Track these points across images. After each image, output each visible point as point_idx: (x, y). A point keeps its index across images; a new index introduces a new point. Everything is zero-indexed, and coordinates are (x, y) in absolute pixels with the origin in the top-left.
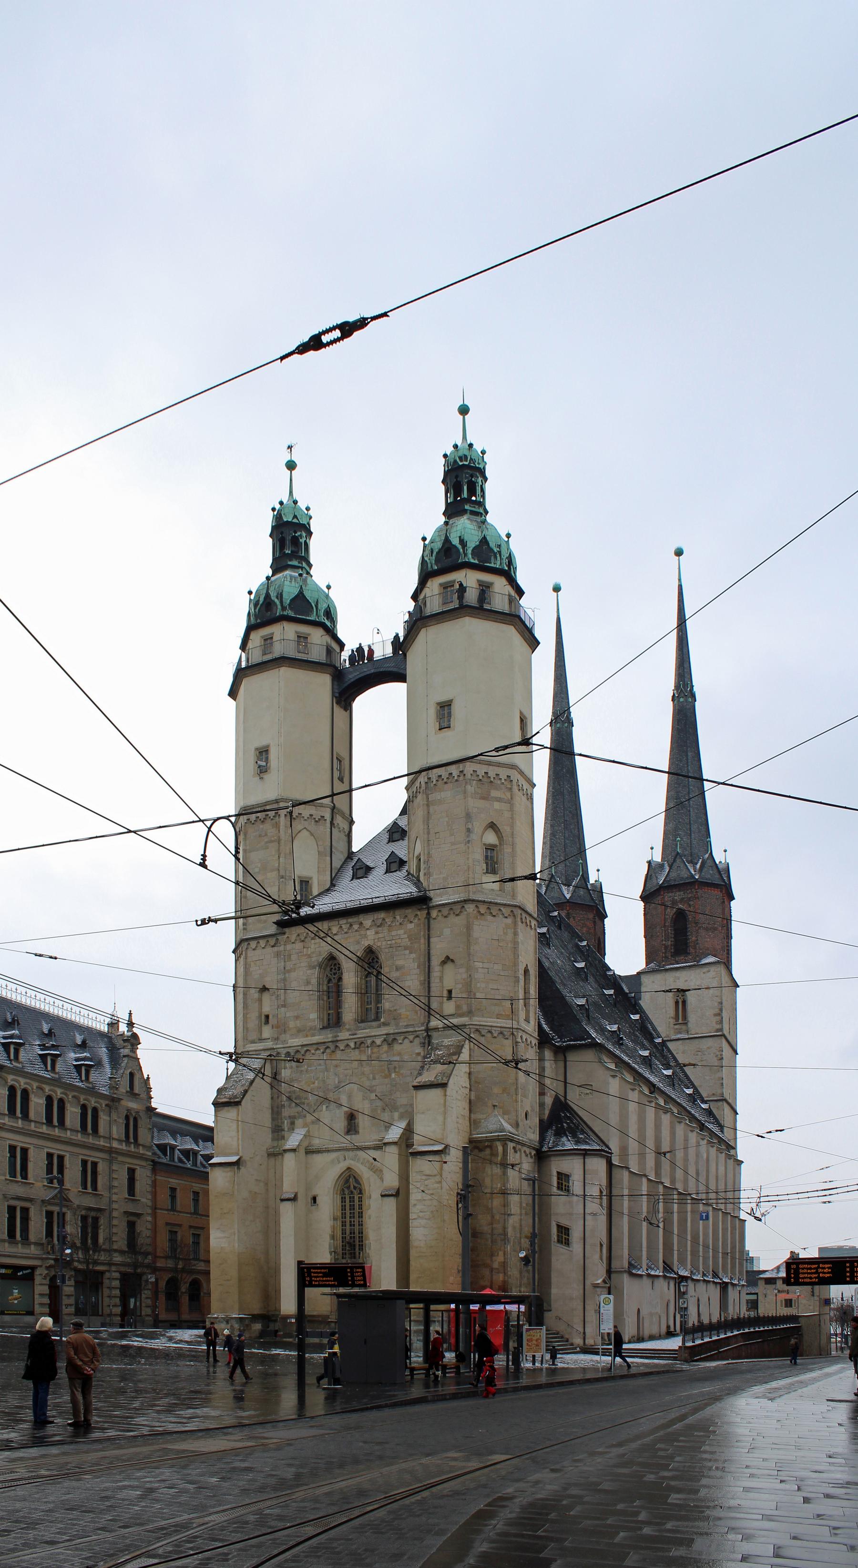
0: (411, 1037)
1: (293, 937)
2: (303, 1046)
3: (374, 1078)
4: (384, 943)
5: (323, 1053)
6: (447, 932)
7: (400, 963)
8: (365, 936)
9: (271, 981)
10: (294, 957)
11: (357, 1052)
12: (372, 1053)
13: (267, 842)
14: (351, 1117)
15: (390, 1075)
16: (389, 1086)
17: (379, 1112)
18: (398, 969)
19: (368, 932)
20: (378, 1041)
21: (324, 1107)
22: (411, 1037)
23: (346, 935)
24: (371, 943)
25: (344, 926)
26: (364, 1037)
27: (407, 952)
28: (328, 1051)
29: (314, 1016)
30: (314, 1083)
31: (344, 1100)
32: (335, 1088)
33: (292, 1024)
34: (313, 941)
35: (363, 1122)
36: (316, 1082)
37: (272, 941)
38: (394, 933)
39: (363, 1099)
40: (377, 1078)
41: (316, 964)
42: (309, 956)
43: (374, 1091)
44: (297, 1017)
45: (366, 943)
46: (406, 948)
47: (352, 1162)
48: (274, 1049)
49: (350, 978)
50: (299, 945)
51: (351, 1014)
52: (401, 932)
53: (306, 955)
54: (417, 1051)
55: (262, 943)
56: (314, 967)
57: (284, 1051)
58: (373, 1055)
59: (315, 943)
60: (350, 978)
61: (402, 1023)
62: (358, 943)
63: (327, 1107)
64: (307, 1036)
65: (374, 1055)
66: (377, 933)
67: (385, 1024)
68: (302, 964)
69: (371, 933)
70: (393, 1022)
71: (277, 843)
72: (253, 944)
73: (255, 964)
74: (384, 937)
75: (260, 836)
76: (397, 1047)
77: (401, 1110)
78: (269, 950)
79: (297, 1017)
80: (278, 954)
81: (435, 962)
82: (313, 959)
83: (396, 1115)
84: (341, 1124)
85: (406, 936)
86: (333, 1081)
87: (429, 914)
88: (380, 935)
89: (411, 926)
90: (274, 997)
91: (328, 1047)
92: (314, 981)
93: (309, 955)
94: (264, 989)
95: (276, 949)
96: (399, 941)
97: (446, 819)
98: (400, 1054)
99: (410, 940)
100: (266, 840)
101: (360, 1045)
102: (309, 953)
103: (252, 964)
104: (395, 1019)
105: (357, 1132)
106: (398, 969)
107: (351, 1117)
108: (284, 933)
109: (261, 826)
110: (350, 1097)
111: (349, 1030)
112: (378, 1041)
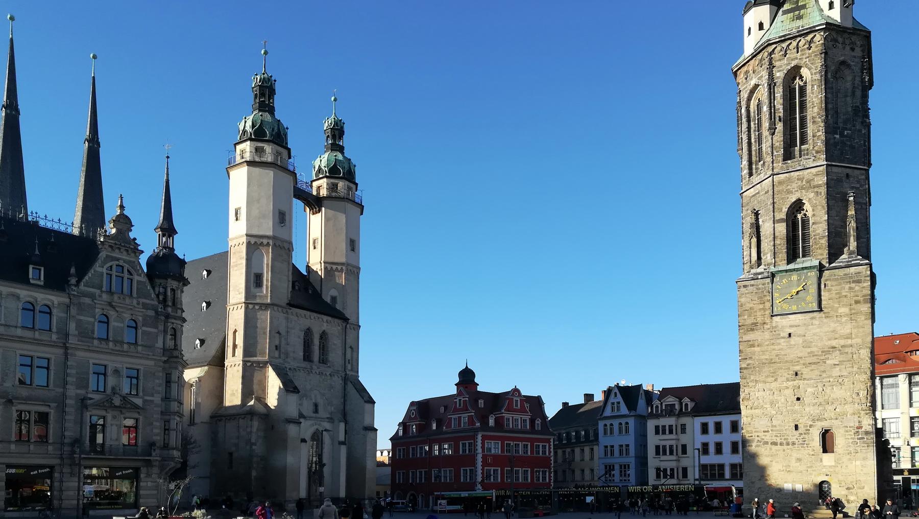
1: (294, 313)
7: (335, 342)
8: (323, 325)
11: (318, 376)
14: (316, 405)
18: (334, 345)
19: (324, 324)
20: (328, 374)
21: (305, 398)
25: (316, 317)
29: (302, 354)
31: (313, 396)
33: (291, 354)
35: (320, 408)
37: (285, 311)
38: (333, 328)
46: (337, 337)
47: (319, 427)
49: (316, 341)
55: (280, 309)
56: (302, 331)
57: (289, 367)
60: (316, 341)
66: (327, 325)
67: (329, 367)
69: (325, 324)
72: (276, 308)
76: (334, 379)
80: (287, 319)
84: (312, 408)
87: (346, 326)
89: (339, 328)
92: (302, 337)
94: (278, 333)
101: (321, 374)
106: (334, 344)
107: (316, 405)
108: (290, 309)
110: (316, 396)
111: (316, 365)
112: (328, 374)
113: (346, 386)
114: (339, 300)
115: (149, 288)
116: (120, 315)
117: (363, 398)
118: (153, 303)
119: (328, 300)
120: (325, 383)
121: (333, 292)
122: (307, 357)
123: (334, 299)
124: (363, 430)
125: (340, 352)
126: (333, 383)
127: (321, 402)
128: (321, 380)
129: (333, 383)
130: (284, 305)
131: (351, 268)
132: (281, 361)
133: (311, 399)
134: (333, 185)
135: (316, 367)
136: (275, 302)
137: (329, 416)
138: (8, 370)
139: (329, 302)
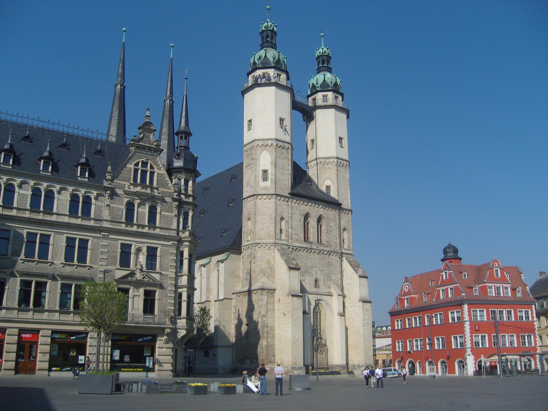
0: (336, 254)
2: (299, 247)
3: (324, 267)
4: (326, 215)
5: (306, 252)
6: (344, 218)
7: (331, 225)
9: (285, 216)
10: (294, 209)
12: (323, 257)
13: (284, 157)
14: (316, 281)
15: (329, 267)
16: (329, 271)
17: (326, 280)
21: (307, 275)
22: (336, 254)
23: (314, 208)
24: (322, 214)
26: (322, 250)
27: (333, 221)
28: (308, 252)
30: (303, 264)
31: (314, 273)
32: (311, 267)
34: (302, 205)
35: (321, 283)
36: (304, 263)
37: (287, 199)
38: (329, 213)
39: (321, 274)
40: (325, 266)
41: (303, 215)
42: (300, 211)
43: (324, 272)
44: (296, 234)
45: (320, 213)
48: (288, 245)
50: (296, 205)
51: (316, 239)
52: (331, 213)
53: (299, 210)
54: (337, 260)
55: (283, 198)
56: (302, 216)
58: (323, 258)
59: (302, 206)
61: (333, 248)
62: (317, 212)
63: (308, 275)
64: (300, 243)
65: (323, 258)
66: (323, 210)
68: (298, 213)
70: (329, 246)
71: (288, 160)
72: (279, 198)
73: (279, 206)
74: (326, 213)
75: (281, 154)
77: (333, 281)
78: (285, 202)
79: (296, 234)
80: (288, 205)
81: (342, 228)
82: (302, 213)
83: (332, 283)
84: (313, 283)
85: (332, 215)
86: (310, 264)
88: (325, 212)
90: (286, 223)
91: (308, 250)
93: (300, 210)
95: (287, 203)
96: (330, 216)
97: (342, 178)
98: (332, 260)
99: (334, 217)
100: (284, 156)
102: (300, 209)
103: (278, 205)
104: (330, 245)
105: (318, 287)
109: (282, 150)
110: (316, 272)
111: (315, 245)
112: (326, 253)
113: (342, 262)
114: (332, 188)
115: (166, 179)
116: (143, 202)
117: (357, 273)
118: (169, 191)
119: (324, 189)
120: (324, 260)
121: (328, 183)
122: (306, 239)
123: (328, 187)
124: (359, 302)
125: (336, 233)
126: (331, 261)
127: (321, 277)
128: (320, 258)
129: (331, 261)
130: (286, 194)
131: (341, 161)
132: (286, 243)
133: (312, 275)
134: (324, 96)
135: (315, 247)
136: (278, 193)
137: (328, 290)
138: (58, 250)
139: (324, 191)
